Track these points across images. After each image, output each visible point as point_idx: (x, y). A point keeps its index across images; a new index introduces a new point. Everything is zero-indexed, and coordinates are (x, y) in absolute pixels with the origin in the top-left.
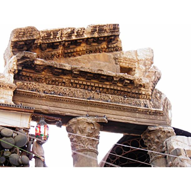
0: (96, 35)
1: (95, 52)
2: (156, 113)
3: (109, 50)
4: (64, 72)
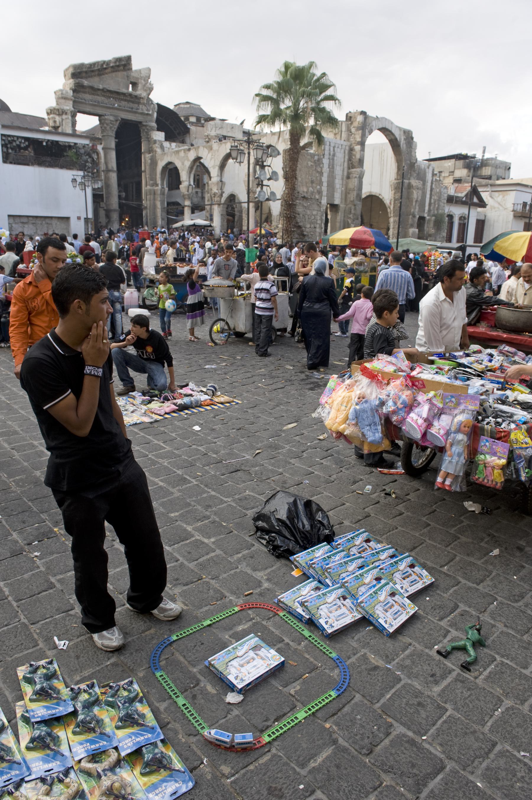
0: (118, 64)
1: (116, 71)
2: (148, 114)
3: (124, 70)
4: (99, 90)
